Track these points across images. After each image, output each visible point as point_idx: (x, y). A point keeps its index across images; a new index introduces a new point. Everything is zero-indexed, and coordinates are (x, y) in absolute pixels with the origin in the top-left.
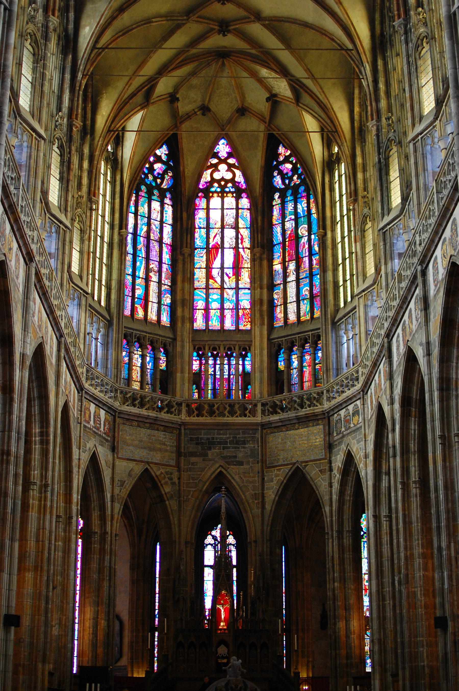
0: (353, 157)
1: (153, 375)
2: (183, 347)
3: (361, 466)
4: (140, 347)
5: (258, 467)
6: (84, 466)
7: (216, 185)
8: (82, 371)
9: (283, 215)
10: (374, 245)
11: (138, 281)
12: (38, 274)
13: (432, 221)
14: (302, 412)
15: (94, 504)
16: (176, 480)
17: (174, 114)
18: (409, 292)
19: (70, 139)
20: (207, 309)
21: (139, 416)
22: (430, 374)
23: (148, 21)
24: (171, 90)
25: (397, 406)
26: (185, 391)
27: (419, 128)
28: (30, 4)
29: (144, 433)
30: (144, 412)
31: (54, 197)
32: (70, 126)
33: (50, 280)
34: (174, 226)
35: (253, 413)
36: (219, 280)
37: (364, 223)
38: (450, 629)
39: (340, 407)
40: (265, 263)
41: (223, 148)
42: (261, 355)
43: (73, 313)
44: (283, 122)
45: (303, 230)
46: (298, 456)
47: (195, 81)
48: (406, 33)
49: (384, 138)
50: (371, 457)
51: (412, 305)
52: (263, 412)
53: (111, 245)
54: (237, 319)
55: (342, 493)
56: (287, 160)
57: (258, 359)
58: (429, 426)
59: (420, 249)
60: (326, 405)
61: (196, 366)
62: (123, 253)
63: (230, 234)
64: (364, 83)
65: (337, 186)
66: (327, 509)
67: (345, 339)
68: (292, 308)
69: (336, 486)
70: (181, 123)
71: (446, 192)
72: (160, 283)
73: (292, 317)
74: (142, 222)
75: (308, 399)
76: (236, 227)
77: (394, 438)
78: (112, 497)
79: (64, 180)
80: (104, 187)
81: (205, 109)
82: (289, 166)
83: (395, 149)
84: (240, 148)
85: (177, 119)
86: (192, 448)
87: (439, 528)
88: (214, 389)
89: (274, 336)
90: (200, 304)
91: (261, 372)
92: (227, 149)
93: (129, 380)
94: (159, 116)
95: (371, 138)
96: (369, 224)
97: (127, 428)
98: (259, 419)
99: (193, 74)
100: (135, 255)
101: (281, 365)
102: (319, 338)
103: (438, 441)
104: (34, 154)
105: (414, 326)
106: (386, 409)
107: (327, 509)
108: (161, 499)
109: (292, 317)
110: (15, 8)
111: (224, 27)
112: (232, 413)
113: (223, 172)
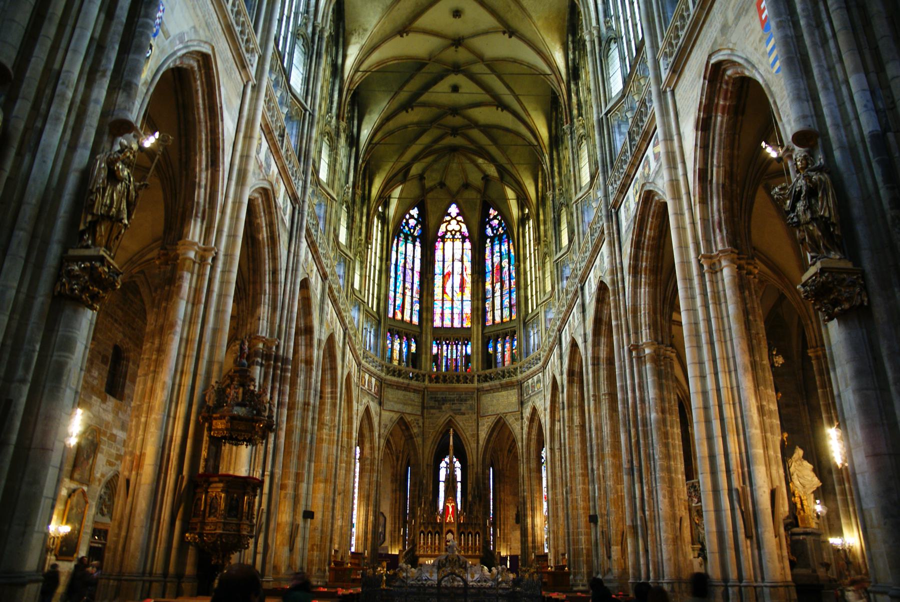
0: (538, 215)
1: (407, 356)
2: (426, 338)
3: (542, 416)
4: (399, 337)
5: (475, 416)
6: (360, 414)
7: (449, 233)
8: (360, 353)
9: (492, 254)
10: (551, 272)
11: (398, 295)
12: (330, 288)
13: (588, 254)
14: (504, 381)
16: (421, 424)
17: (423, 187)
18: (573, 301)
19: (354, 202)
20: (442, 314)
21: (398, 382)
22: (586, 354)
23: (405, 127)
24: (420, 172)
25: (565, 376)
27: (580, 195)
28: (328, 113)
29: (400, 393)
30: (401, 380)
31: (343, 239)
32: (354, 193)
33: (339, 292)
35: (472, 382)
36: (450, 294)
37: (544, 258)
38: (599, 523)
40: (480, 284)
41: (453, 210)
42: (477, 343)
43: (355, 315)
44: (493, 194)
45: (505, 263)
46: (501, 410)
47: (436, 166)
48: (571, 133)
49: (557, 203)
50: (548, 410)
51: (575, 310)
52: (478, 381)
53: (380, 272)
55: (529, 433)
56: (495, 217)
57: (475, 346)
58: (585, 389)
59: (580, 273)
60: (520, 377)
61: (435, 350)
62: (388, 277)
63: (458, 265)
64: (545, 167)
65: (527, 235)
66: (520, 444)
68: (498, 313)
70: (427, 193)
71: (596, 235)
72: (412, 296)
73: (498, 319)
75: (508, 372)
76: (462, 261)
77: (563, 397)
78: (379, 435)
79: (350, 228)
81: (442, 185)
82: (496, 222)
83: (564, 209)
84: (465, 210)
85: (424, 191)
86: (432, 403)
87: (592, 456)
88: (447, 366)
89: (486, 331)
90: (438, 310)
91: (478, 354)
92: (457, 211)
93: (391, 359)
94: (413, 189)
95: (549, 203)
96: (548, 259)
97: (389, 390)
98: (476, 384)
99: (435, 161)
100: (396, 279)
101: (491, 350)
102: (515, 332)
103: (591, 398)
104: (329, 210)
105: (576, 324)
106: (558, 378)
107: (520, 444)
109: (498, 319)
110: (317, 114)
111: (455, 131)
112: (458, 381)
113: (454, 226)
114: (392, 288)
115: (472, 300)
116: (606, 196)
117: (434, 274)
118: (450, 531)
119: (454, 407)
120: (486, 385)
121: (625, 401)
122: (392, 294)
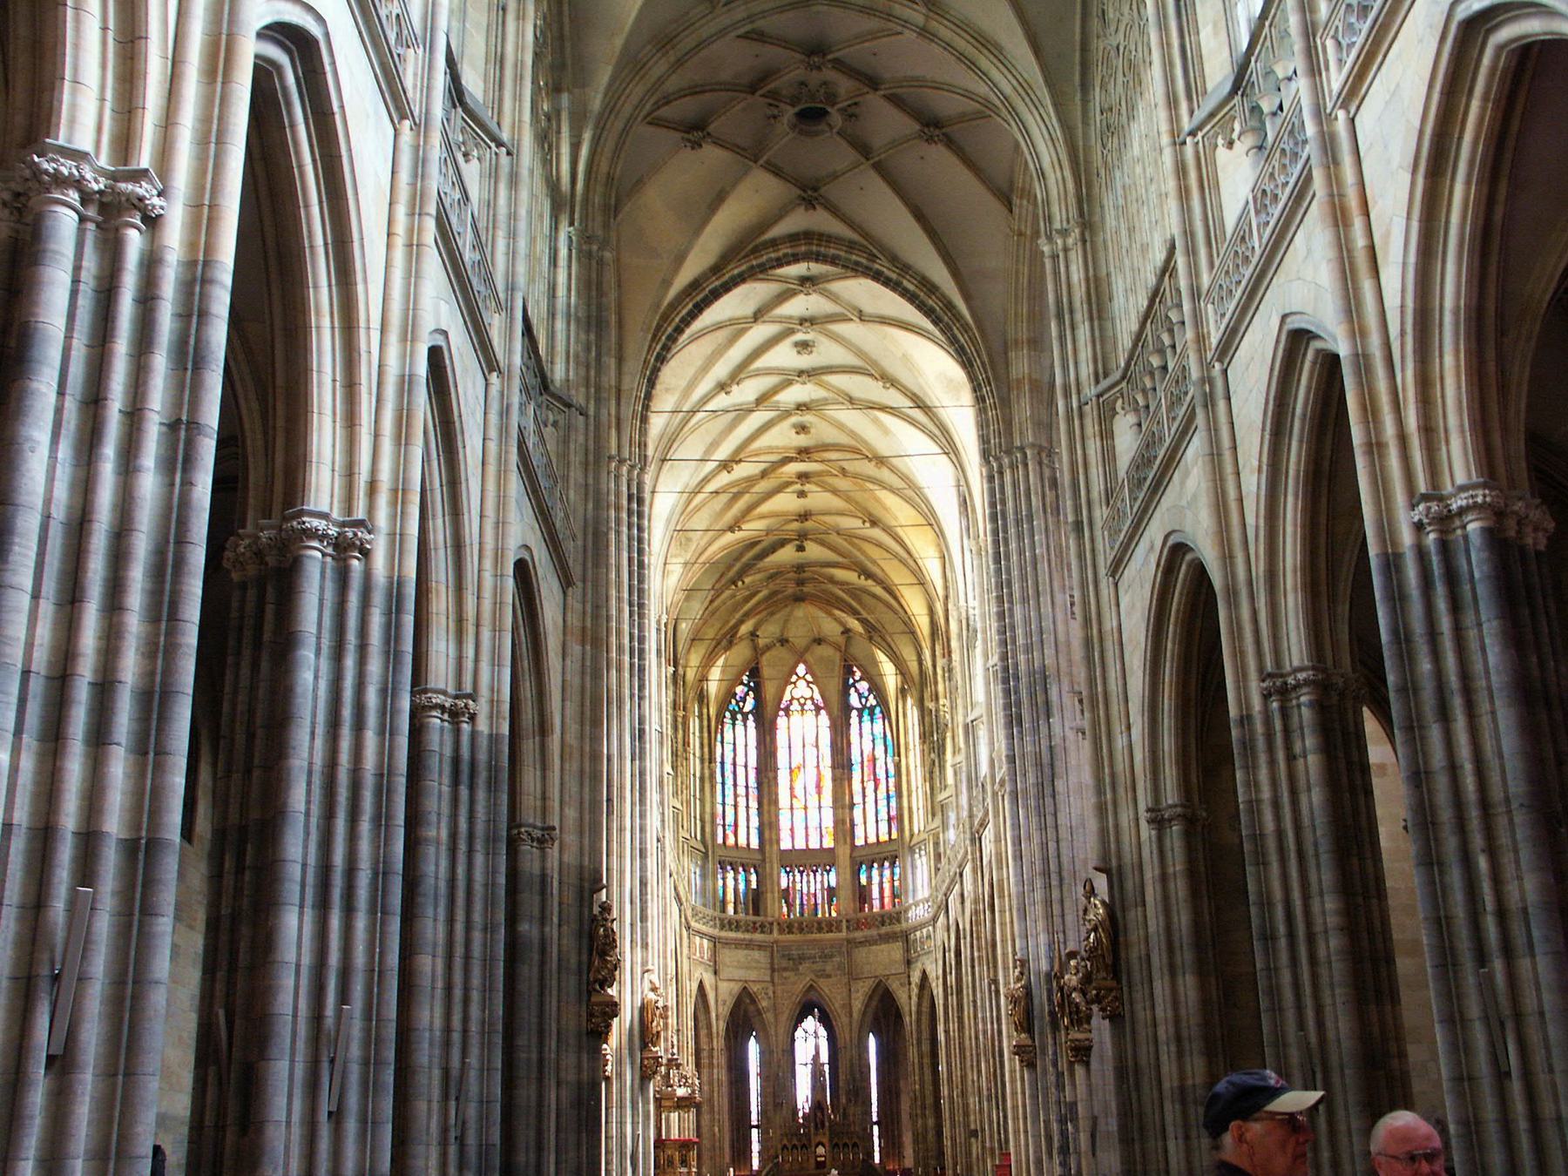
1: (746, 894)
14: (884, 930)
15: (702, 1024)
17: (755, 648)
20: (792, 830)
23: (733, 596)
29: (741, 954)
30: (740, 935)
34: (758, 748)
39: (915, 929)
44: (859, 647)
53: (702, 779)
55: (919, 1005)
60: (904, 925)
61: (784, 885)
62: (713, 787)
67: (918, 862)
69: (914, 999)
74: (728, 748)
80: (694, 725)
81: (783, 641)
82: (863, 686)
85: (758, 652)
86: (784, 963)
88: (802, 904)
97: (726, 951)
98: (844, 934)
100: (723, 784)
101: (864, 881)
108: (759, 1012)
112: (820, 930)
114: (719, 798)
115: (835, 808)
116: (971, 816)
117: (776, 770)
119: (815, 967)
121: (985, 1032)
122: (719, 808)
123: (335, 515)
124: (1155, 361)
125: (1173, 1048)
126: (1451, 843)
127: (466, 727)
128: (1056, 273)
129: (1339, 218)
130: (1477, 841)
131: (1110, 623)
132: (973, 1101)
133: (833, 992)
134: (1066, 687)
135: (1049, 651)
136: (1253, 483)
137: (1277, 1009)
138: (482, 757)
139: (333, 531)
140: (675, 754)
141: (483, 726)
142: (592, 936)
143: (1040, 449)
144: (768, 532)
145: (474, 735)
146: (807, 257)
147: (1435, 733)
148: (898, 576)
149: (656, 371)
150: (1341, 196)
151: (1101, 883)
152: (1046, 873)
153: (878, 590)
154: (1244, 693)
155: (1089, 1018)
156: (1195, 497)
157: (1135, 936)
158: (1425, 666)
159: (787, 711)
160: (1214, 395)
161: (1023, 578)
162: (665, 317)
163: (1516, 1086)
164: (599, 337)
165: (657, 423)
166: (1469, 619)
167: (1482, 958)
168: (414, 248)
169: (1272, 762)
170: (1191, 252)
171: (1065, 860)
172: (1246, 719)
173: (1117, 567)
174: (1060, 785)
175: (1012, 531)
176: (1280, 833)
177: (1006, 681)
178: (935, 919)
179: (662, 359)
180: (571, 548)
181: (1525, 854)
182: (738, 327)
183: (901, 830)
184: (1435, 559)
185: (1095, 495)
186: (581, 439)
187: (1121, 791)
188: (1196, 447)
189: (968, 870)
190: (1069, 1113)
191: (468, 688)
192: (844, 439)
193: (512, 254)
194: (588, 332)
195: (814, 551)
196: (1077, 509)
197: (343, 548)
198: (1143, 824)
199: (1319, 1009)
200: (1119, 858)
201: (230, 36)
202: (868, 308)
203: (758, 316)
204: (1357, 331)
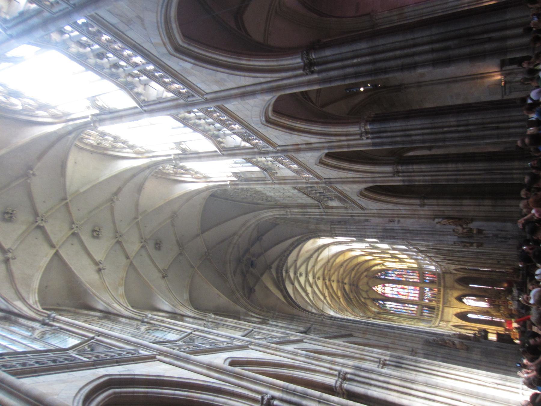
9: (391, 277)
26: (434, 304)
29: (445, 314)
52: (440, 286)
54: (417, 290)
63: (394, 289)
76: (393, 288)
80: (386, 316)
81: (367, 292)
82: (379, 274)
90: (412, 298)
94: (369, 302)
107: (466, 276)
108: (461, 313)
109: (417, 277)
111: (353, 285)
112: (440, 294)
116: (415, 252)
117: (398, 298)
118: (499, 302)
120: (442, 284)
123: (336, 379)
124: (318, 195)
125: (481, 207)
126: (440, 136)
127: (387, 362)
128: (295, 215)
129: (298, 150)
130: (440, 130)
131: (375, 211)
132: (490, 261)
133: (456, 294)
134: (387, 225)
135: (378, 228)
136: (350, 175)
137: (475, 180)
138: (395, 360)
139: (340, 380)
140: (392, 321)
141: (387, 358)
142: (441, 345)
143: (331, 225)
144: (341, 290)
145: (389, 361)
146: (282, 270)
147: (414, 138)
148: (355, 262)
149: (302, 309)
150: (294, 149)
151: (437, 220)
152: (433, 234)
153: (358, 267)
154: (397, 181)
155: (471, 229)
156: (350, 188)
157: (451, 214)
158: (398, 139)
159: (384, 293)
160: (329, 182)
161: (361, 231)
162: (291, 305)
163: (501, 125)
164: (295, 318)
165: (314, 311)
166: (389, 129)
167: (468, 131)
168: (277, 350)
169: (414, 176)
170: (298, 183)
171: (429, 230)
172: (403, 181)
173: (362, 208)
174: (410, 229)
175: (349, 233)
176: (432, 176)
177: (384, 238)
178: (440, 265)
179: (300, 307)
180: (344, 332)
181: (444, 120)
182: (295, 289)
183: (416, 270)
184: (375, 135)
185: (345, 212)
186: (318, 326)
187: (415, 213)
188: (339, 187)
189: (429, 255)
190: (496, 236)
191: (378, 360)
192: (322, 269)
193: (277, 332)
194: (293, 320)
195: (346, 281)
196: (348, 216)
197: (345, 379)
198: (423, 209)
199: (476, 170)
200: (430, 215)
201: (234, 373)
202: (294, 258)
203: (293, 284)
204: (323, 148)
